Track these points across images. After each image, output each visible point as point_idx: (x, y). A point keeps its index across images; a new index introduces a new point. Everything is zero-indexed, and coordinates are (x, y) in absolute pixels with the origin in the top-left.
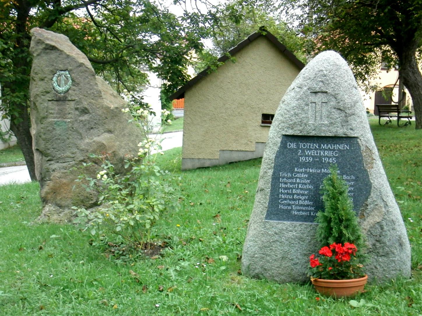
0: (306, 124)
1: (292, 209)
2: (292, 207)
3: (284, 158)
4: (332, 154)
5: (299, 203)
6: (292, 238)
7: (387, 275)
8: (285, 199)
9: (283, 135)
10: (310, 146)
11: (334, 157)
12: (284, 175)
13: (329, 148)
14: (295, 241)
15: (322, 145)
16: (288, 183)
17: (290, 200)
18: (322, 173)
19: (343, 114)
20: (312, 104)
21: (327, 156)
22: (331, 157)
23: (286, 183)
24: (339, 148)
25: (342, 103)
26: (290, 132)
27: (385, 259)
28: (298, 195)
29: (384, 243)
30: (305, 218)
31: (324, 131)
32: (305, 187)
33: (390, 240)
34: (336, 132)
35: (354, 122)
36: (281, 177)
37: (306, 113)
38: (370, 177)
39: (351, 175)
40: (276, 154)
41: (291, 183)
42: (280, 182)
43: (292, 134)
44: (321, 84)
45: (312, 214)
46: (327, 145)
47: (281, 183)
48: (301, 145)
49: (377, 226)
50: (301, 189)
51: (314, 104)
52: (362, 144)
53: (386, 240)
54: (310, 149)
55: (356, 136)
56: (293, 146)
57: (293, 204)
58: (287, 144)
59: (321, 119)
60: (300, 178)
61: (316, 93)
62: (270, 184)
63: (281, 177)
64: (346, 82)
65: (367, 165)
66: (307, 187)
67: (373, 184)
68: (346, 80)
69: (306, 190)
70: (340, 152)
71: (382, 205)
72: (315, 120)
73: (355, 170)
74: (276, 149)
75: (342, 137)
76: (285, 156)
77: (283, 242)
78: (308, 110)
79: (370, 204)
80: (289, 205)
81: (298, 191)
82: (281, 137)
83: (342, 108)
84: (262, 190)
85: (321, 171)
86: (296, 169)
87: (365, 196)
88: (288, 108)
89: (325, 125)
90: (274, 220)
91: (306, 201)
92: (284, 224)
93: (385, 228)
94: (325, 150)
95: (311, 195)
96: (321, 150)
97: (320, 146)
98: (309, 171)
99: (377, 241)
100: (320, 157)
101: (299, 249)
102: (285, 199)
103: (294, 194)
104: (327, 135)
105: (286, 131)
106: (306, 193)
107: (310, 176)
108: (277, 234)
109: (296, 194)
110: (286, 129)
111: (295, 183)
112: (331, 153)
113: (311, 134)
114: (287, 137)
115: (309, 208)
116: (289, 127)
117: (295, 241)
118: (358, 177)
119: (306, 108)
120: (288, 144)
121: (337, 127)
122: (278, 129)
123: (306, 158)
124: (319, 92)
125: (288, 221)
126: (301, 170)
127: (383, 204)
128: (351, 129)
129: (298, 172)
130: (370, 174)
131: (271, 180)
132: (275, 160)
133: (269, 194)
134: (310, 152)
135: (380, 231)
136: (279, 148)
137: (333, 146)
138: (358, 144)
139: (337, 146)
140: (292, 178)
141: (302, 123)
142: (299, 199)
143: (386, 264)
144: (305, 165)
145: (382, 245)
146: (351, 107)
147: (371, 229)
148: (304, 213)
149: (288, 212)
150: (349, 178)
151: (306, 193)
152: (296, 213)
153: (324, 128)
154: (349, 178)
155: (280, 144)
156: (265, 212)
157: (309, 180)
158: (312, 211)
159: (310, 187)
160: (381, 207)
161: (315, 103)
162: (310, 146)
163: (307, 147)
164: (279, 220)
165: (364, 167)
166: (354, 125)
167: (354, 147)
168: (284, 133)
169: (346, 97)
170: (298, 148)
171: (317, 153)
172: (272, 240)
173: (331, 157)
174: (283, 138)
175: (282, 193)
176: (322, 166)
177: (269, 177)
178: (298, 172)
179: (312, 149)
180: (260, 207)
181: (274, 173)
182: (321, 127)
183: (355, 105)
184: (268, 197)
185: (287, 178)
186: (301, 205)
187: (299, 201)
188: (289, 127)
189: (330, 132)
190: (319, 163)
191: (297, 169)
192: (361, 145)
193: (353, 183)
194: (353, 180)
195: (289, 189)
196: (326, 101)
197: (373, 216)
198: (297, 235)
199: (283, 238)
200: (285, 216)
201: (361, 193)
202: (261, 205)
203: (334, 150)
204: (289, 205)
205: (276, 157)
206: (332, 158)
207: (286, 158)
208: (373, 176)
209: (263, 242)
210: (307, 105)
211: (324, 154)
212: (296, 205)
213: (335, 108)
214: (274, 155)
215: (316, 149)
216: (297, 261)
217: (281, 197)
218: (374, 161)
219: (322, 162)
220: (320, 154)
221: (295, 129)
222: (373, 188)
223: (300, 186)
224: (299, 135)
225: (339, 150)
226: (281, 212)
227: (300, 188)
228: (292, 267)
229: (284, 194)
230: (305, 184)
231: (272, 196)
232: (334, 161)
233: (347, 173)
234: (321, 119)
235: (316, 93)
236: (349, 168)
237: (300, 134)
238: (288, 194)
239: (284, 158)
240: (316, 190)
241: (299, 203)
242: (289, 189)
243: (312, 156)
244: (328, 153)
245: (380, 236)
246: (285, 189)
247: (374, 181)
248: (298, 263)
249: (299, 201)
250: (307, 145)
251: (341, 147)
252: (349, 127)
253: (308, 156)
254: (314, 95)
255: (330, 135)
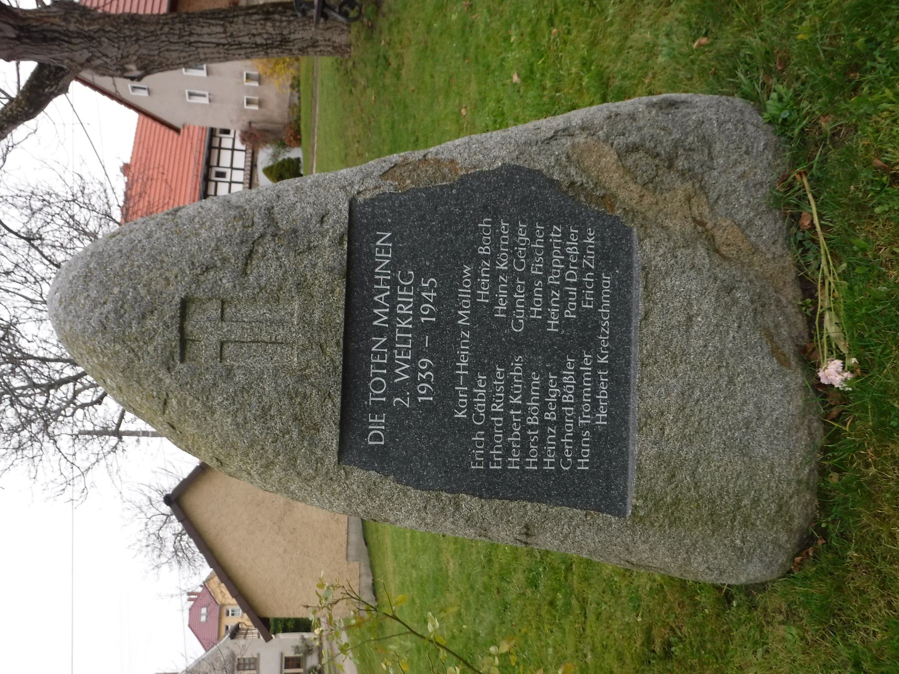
0: (303, 378)
1: (591, 427)
2: (585, 427)
3: (421, 458)
4: (409, 288)
5: (571, 405)
6: (685, 427)
7: (761, 148)
8: (560, 450)
9: (339, 461)
10: (379, 366)
11: (416, 284)
12: (480, 455)
13: (387, 299)
14: (693, 415)
15: (375, 323)
16: (505, 441)
17: (561, 434)
18: (473, 324)
19: (268, 246)
20: (226, 352)
21: (416, 308)
22: (418, 295)
23: (507, 449)
24: (387, 267)
25: (227, 250)
26: (330, 435)
27: (718, 147)
28: (544, 407)
29: (676, 147)
30: (618, 382)
31: (325, 313)
32: (518, 384)
33: (664, 129)
34: (331, 270)
35: (297, 211)
36: (487, 465)
37: (261, 379)
38: (486, 168)
39: (477, 228)
40: (407, 485)
41: (508, 431)
42: (505, 469)
43: (336, 430)
44: (150, 323)
45: (602, 361)
46: (378, 305)
47: (505, 464)
48: (376, 396)
49: (629, 162)
50: (526, 397)
51: (229, 349)
52: (376, 188)
53: (667, 142)
54: (391, 365)
55: (346, 205)
56: (377, 425)
57: (576, 423)
58: (373, 447)
59: (282, 323)
60: (489, 402)
61: (184, 341)
62: (512, 505)
63: (487, 465)
64: (149, 236)
65: (444, 178)
66: (519, 378)
67: (507, 160)
68: (140, 236)
69: (527, 380)
70: (400, 261)
71: (567, 142)
72: (283, 343)
73: (463, 214)
74: (389, 485)
75: (350, 253)
76: (415, 453)
77: (696, 454)
78: (248, 371)
79: (568, 175)
80: (577, 437)
81: (533, 405)
82: (348, 468)
83: (245, 249)
84: (528, 531)
85: (465, 328)
86: (460, 415)
87: (545, 187)
88: (242, 445)
89: (304, 308)
90: (626, 487)
91: (565, 380)
92: (640, 453)
93: (634, 138)
94: (392, 314)
95: (544, 363)
96: (393, 329)
97: (380, 332)
98: (464, 368)
99: (670, 167)
100: (419, 329)
101: (716, 403)
102: (560, 450)
103: (542, 420)
104: (342, 303)
105: (326, 449)
106: (536, 380)
107: (483, 364)
108: (674, 476)
109: (541, 416)
110: (319, 453)
111: (508, 419)
112: (405, 293)
113: (339, 359)
114: (351, 444)
115: (587, 369)
116: (312, 438)
117: (693, 415)
118: (485, 207)
119: (239, 377)
120: (370, 443)
121: (314, 266)
122: (319, 480)
123: (423, 381)
124: (182, 330)
125: (626, 439)
126: (463, 399)
127: (564, 140)
128: (322, 221)
129: (471, 406)
130: (475, 167)
131: (497, 501)
132: (428, 489)
133: (544, 507)
134: (400, 367)
135: (641, 154)
136: (387, 476)
137: (381, 287)
138: (372, 199)
139: (381, 272)
140: (489, 428)
141: (297, 394)
142: (559, 403)
143: (731, 146)
144: (445, 383)
145: (681, 151)
146: (241, 217)
147: (639, 180)
148: (604, 389)
149: (599, 439)
150: (487, 236)
151: (536, 380)
152: (603, 414)
153: (317, 315)
154: (487, 236)
155: (373, 473)
156: (601, 518)
157: (495, 371)
158: (595, 359)
159: (518, 366)
160: (573, 146)
161: (222, 344)
162: (379, 366)
163: (382, 375)
164: (625, 469)
165: (451, 187)
166: (309, 210)
167: (384, 215)
168: (332, 458)
169: (204, 234)
170: (387, 406)
171: (405, 341)
172: (693, 492)
173: (418, 295)
174: (350, 463)
175: (540, 463)
176: (447, 323)
177: (486, 507)
178: (471, 406)
179: (391, 358)
180: (582, 534)
181: (473, 491)
182: (310, 323)
183: (238, 207)
184: (554, 511)
185: (490, 444)
186: (578, 395)
187: (566, 405)
188: (312, 438)
189: (332, 292)
190: (437, 338)
191: (460, 410)
192: (377, 191)
193: (504, 225)
194: (495, 224)
195: (525, 438)
196: (215, 305)
197: (601, 171)
198: (673, 409)
199: (683, 454)
200: (614, 452)
201: (536, 198)
202: (578, 533)
203: (393, 283)
204: (577, 437)
205: (416, 488)
206: (423, 289)
207: (421, 449)
208: (480, 161)
209: (697, 522)
210: (230, 371)
211: (408, 316)
212: (578, 412)
213: (244, 273)
214: (412, 492)
215: (390, 345)
216: (751, 406)
217: (552, 464)
218: (429, 156)
219: (435, 325)
220: (406, 330)
221: (317, 418)
222: (520, 163)
223: (516, 401)
224: (339, 405)
225: (393, 266)
226: (602, 464)
227: (522, 399)
228: (768, 424)
229: (542, 454)
230: (509, 382)
231: (549, 496)
232: (432, 284)
233: (473, 243)
234: (282, 323)
235: (184, 341)
236: (457, 233)
237: (338, 400)
238: (542, 442)
239: (421, 458)
240: (528, 346)
241: (571, 405)
242: (525, 438)
243: (416, 357)
244: (403, 304)
245: (658, 155)
246: (525, 451)
247: (496, 158)
248: (756, 404)
249: (566, 405)
250: (375, 375)
251: (384, 259)
252: (314, 225)
253: (414, 371)
254: (192, 349)
255: (340, 290)
